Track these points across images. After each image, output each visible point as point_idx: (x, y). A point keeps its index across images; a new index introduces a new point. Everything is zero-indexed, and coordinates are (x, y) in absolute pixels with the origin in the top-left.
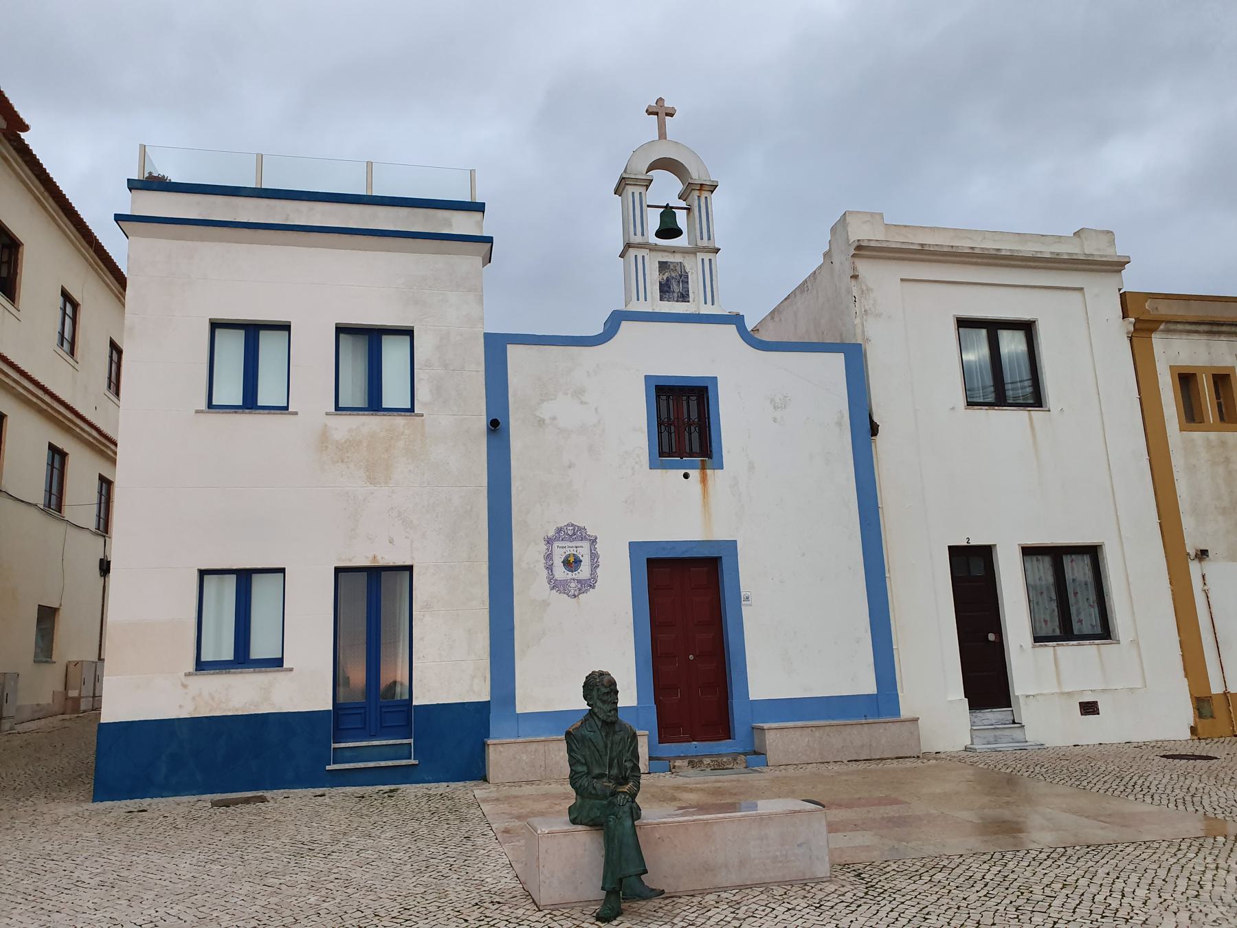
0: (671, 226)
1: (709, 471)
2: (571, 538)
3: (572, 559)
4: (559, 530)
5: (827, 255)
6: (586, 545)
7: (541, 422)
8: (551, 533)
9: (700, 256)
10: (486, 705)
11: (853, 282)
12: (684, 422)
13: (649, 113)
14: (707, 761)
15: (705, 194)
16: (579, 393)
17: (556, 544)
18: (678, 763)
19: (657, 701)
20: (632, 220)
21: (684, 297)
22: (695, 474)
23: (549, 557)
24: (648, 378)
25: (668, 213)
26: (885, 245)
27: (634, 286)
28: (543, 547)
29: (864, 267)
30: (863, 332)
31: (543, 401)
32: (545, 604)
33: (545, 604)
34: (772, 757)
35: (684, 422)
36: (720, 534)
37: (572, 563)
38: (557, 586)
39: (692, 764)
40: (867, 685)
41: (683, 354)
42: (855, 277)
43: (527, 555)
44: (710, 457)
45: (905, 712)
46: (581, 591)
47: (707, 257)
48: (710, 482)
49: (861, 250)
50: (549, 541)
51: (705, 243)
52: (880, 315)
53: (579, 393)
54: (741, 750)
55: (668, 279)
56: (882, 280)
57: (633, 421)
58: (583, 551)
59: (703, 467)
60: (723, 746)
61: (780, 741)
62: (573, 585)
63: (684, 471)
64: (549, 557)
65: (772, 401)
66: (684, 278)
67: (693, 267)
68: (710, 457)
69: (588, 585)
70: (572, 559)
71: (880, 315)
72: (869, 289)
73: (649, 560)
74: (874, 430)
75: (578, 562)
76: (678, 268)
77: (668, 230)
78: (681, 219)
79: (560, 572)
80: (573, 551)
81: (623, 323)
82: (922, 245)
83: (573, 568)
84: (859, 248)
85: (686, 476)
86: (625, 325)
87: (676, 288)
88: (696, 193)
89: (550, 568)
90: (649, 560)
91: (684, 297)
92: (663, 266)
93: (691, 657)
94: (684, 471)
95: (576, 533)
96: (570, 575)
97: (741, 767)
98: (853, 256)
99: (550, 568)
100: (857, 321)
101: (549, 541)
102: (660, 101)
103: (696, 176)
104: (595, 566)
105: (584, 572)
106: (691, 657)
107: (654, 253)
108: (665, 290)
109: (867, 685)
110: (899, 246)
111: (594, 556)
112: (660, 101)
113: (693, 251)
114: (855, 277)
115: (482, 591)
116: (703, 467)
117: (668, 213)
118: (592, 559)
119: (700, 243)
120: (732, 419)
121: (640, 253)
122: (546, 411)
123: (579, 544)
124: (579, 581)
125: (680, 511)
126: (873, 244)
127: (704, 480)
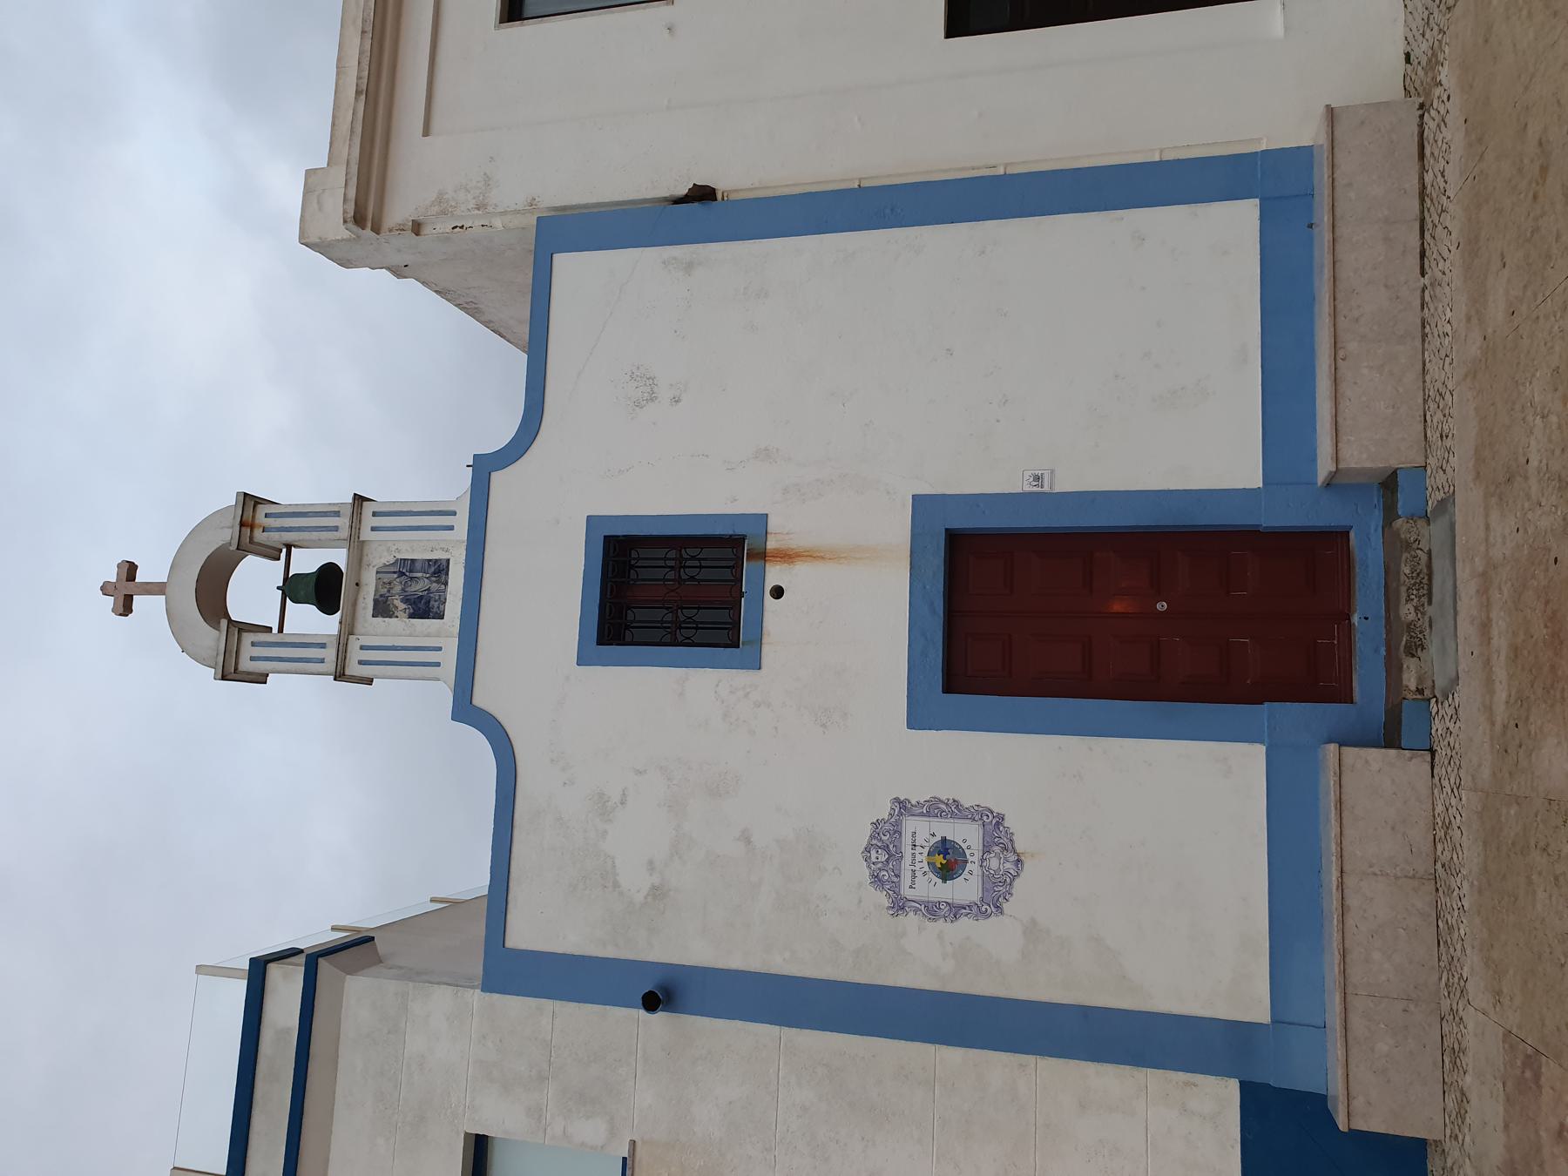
0: (312, 585)
1: (771, 544)
2: (894, 856)
3: (939, 860)
4: (877, 880)
5: (399, 272)
6: (911, 825)
7: (658, 893)
8: (882, 899)
9: (366, 534)
10: (1245, 1087)
11: (427, 230)
12: (672, 591)
13: (126, 608)
14: (1407, 612)
15: (260, 518)
16: (603, 807)
17: (907, 892)
18: (1410, 680)
19: (1255, 697)
21: (439, 570)
22: (775, 575)
23: (932, 910)
24: (582, 660)
25: (293, 588)
26: (354, 168)
27: (417, 664)
28: (911, 920)
29: (399, 210)
30: (517, 212)
31: (616, 885)
32: (1032, 931)
33: (1032, 931)
34: (1399, 452)
35: (672, 591)
36: (897, 529)
37: (948, 861)
38: (994, 900)
39: (1415, 648)
40: (1240, 219)
41: (541, 589)
42: (417, 228)
43: (925, 958)
44: (742, 539)
46: (1008, 847)
47: (368, 521)
48: (795, 543)
49: (364, 215)
50: (899, 906)
51: (343, 522)
52: (487, 179)
53: (603, 807)
54: (1377, 517)
55: (406, 600)
56: (424, 174)
57: (665, 694)
58: (921, 832)
59: (762, 555)
60: (1368, 551)
61: (1362, 430)
62: (994, 864)
63: (768, 599)
64: (932, 910)
65: (638, 404)
66: (405, 568)
67: (386, 548)
68: (742, 539)
69: (995, 828)
70: (939, 860)
71: (487, 179)
72: (440, 199)
73: (948, 688)
74: (703, 194)
75: (944, 847)
76: (386, 578)
77: (324, 589)
78: (306, 562)
79: (965, 888)
80: (922, 856)
81: (477, 701)
82: (358, 93)
83: (961, 859)
84: (359, 219)
85: (778, 592)
86: (478, 700)
87: (418, 588)
88: (259, 536)
89: (956, 911)
90: (948, 688)
91: (439, 570)
92: (382, 608)
93: (1162, 606)
94: (768, 599)
95: (885, 842)
96: (973, 866)
97: (1437, 529)
98: (376, 229)
99: (956, 911)
100: (498, 223)
101: (899, 906)
102: (106, 589)
103: (226, 535)
104: (954, 810)
105: (967, 835)
106: (1162, 606)
107: (359, 627)
108: (424, 608)
109: (1243, 216)
110: (357, 141)
111: (935, 809)
112: (106, 589)
113: (357, 546)
114: (417, 228)
115: (998, 1066)
116: (762, 555)
117: (293, 588)
118: (940, 814)
119: (344, 533)
120: (673, 489)
121: (355, 655)
122: (636, 882)
123: (907, 840)
124: (987, 849)
126: (352, 193)
127: (787, 556)
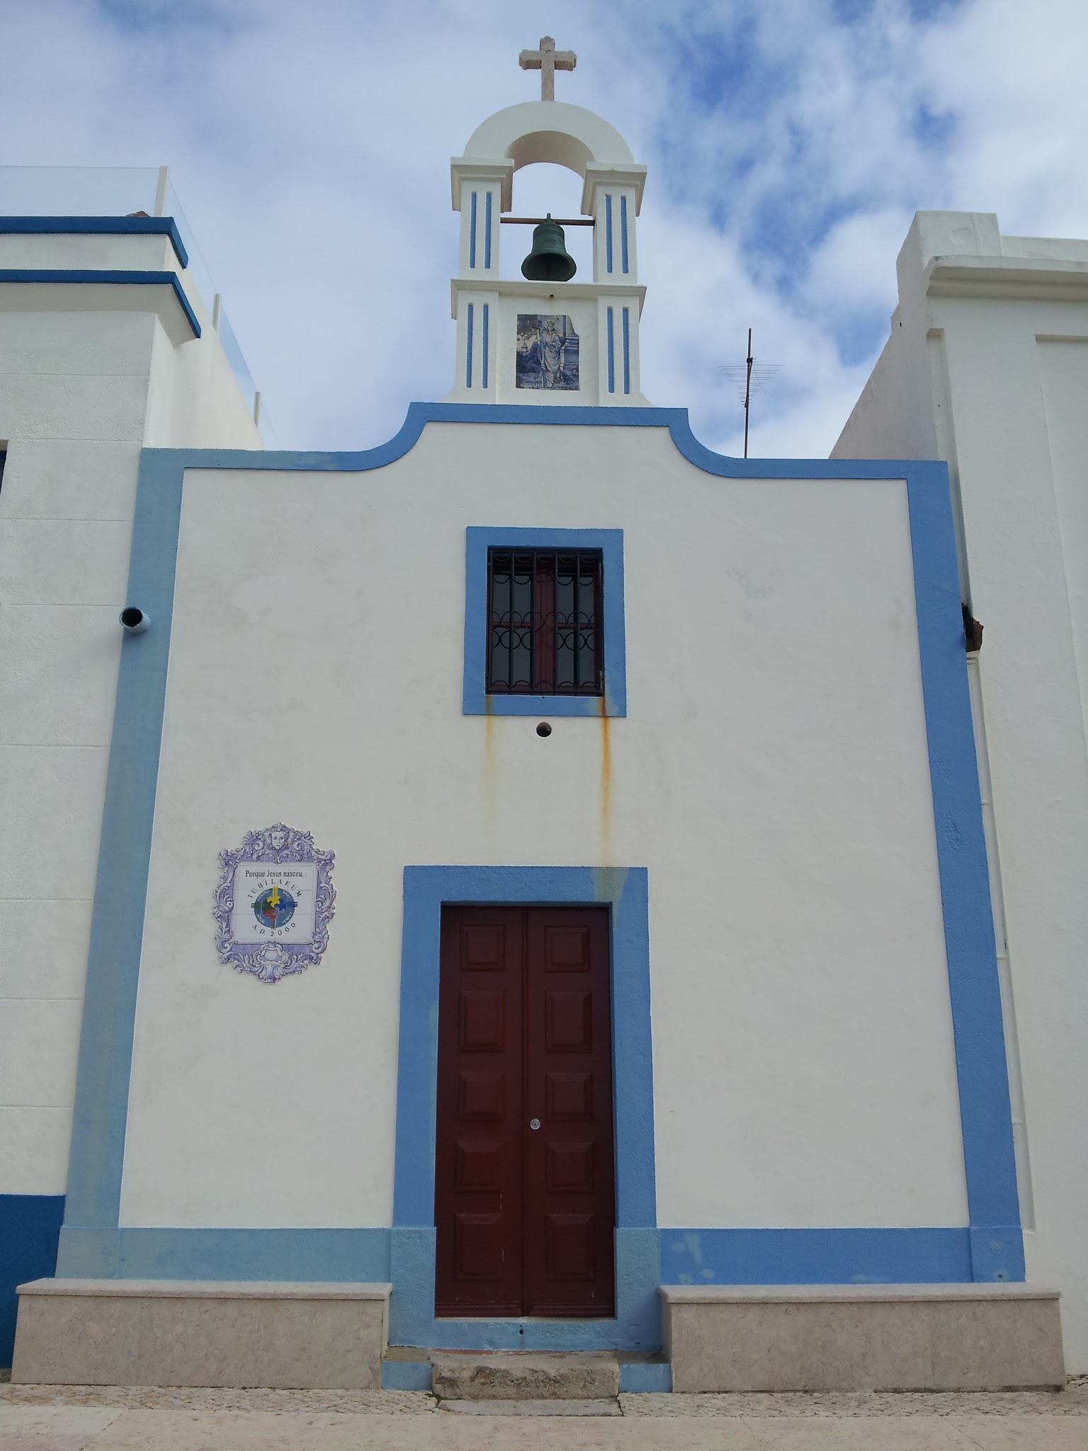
0: (556, 249)
2: (278, 854)
3: (275, 900)
4: (254, 838)
6: (309, 871)
8: (235, 845)
12: (545, 621)
13: (528, 63)
17: (243, 868)
19: (444, 1218)
20: (480, 247)
21: (568, 380)
23: (225, 893)
25: (548, 230)
27: (475, 364)
28: (213, 875)
35: (545, 621)
38: (235, 954)
40: (950, 1211)
41: (545, 487)
43: (179, 890)
45: (1036, 1280)
46: (289, 970)
50: (229, 861)
55: (535, 348)
57: (439, 617)
58: (300, 881)
62: (271, 955)
63: (536, 722)
66: (569, 345)
69: (304, 956)
70: (275, 900)
74: (972, 635)
75: (288, 905)
76: (559, 327)
77: (549, 263)
78: (577, 243)
79: (247, 927)
80: (277, 883)
83: (273, 916)
87: (550, 361)
89: (225, 918)
91: (568, 380)
92: (527, 324)
93: (536, 1124)
94: (536, 722)
95: (290, 845)
96: (268, 934)
99: (225, 918)
101: (229, 861)
102: (547, 42)
104: (324, 915)
105: (299, 927)
106: (536, 1124)
108: (528, 367)
109: (950, 1211)
111: (325, 894)
112: (547, 42)
120: (649, 615)
124: (287, 947)
125: (537, 802)
